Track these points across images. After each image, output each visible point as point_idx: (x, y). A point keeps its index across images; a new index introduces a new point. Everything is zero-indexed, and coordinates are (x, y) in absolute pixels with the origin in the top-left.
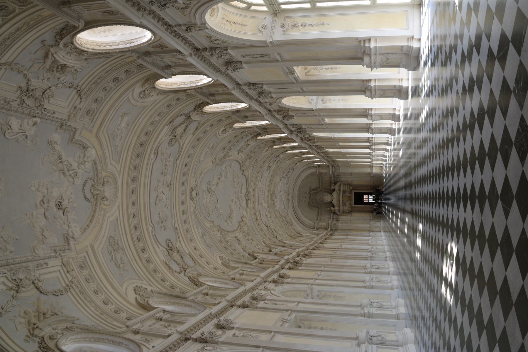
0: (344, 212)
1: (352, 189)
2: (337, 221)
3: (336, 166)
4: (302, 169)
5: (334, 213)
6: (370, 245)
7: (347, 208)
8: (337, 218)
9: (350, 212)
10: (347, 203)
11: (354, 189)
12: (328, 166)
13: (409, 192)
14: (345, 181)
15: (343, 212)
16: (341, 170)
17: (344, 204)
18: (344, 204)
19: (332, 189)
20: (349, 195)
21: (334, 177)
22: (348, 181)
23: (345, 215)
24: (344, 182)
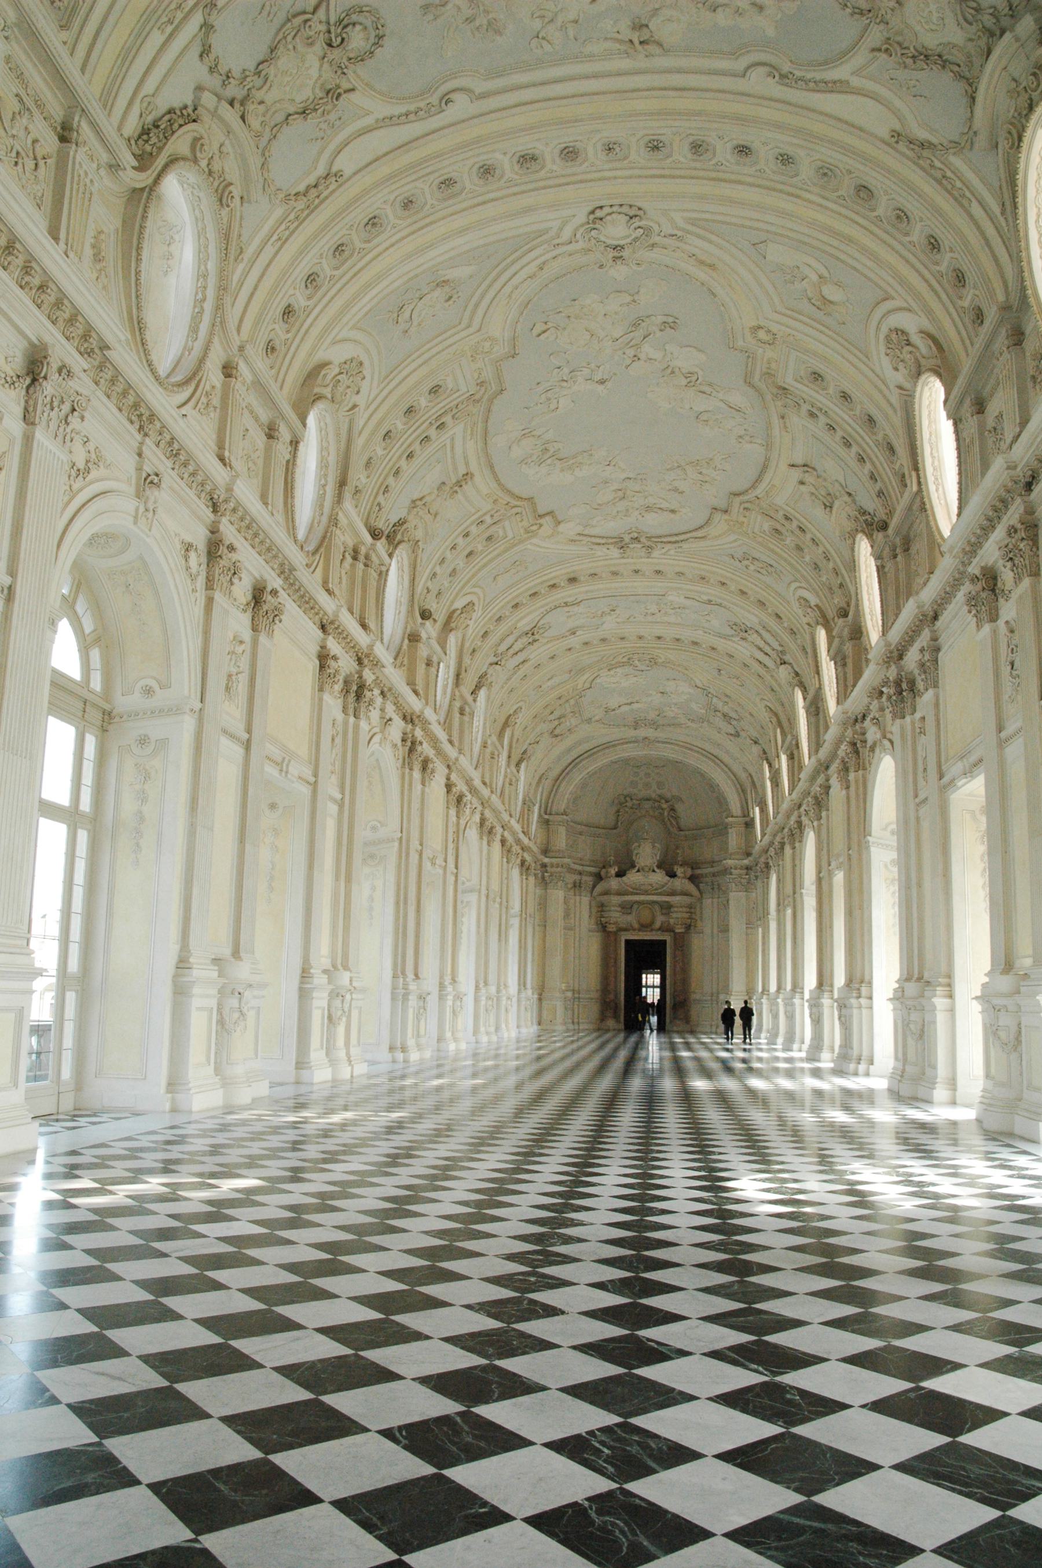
0: (602, 907)
1: (675, 934)
2: (575, 886)
3: (749, 879)
4: (736, 768)
5: (599, 878)
6: (498, 991)
7: (616, 917)
8: (583, 886)
9: (603, 927)
10: (631, 919)
11: (675, 939)
12: (748, 854)
13: (671, 1119)
14: (701, 908)
15: (602, 905)
16: (736, 898)
17: (626, 908)
18: (626, 908)
19: (676, 867)
20: (657, 925)
21: (714, 875)
22: (701, 920)
23: (594, 910)
24: (698, 905)
